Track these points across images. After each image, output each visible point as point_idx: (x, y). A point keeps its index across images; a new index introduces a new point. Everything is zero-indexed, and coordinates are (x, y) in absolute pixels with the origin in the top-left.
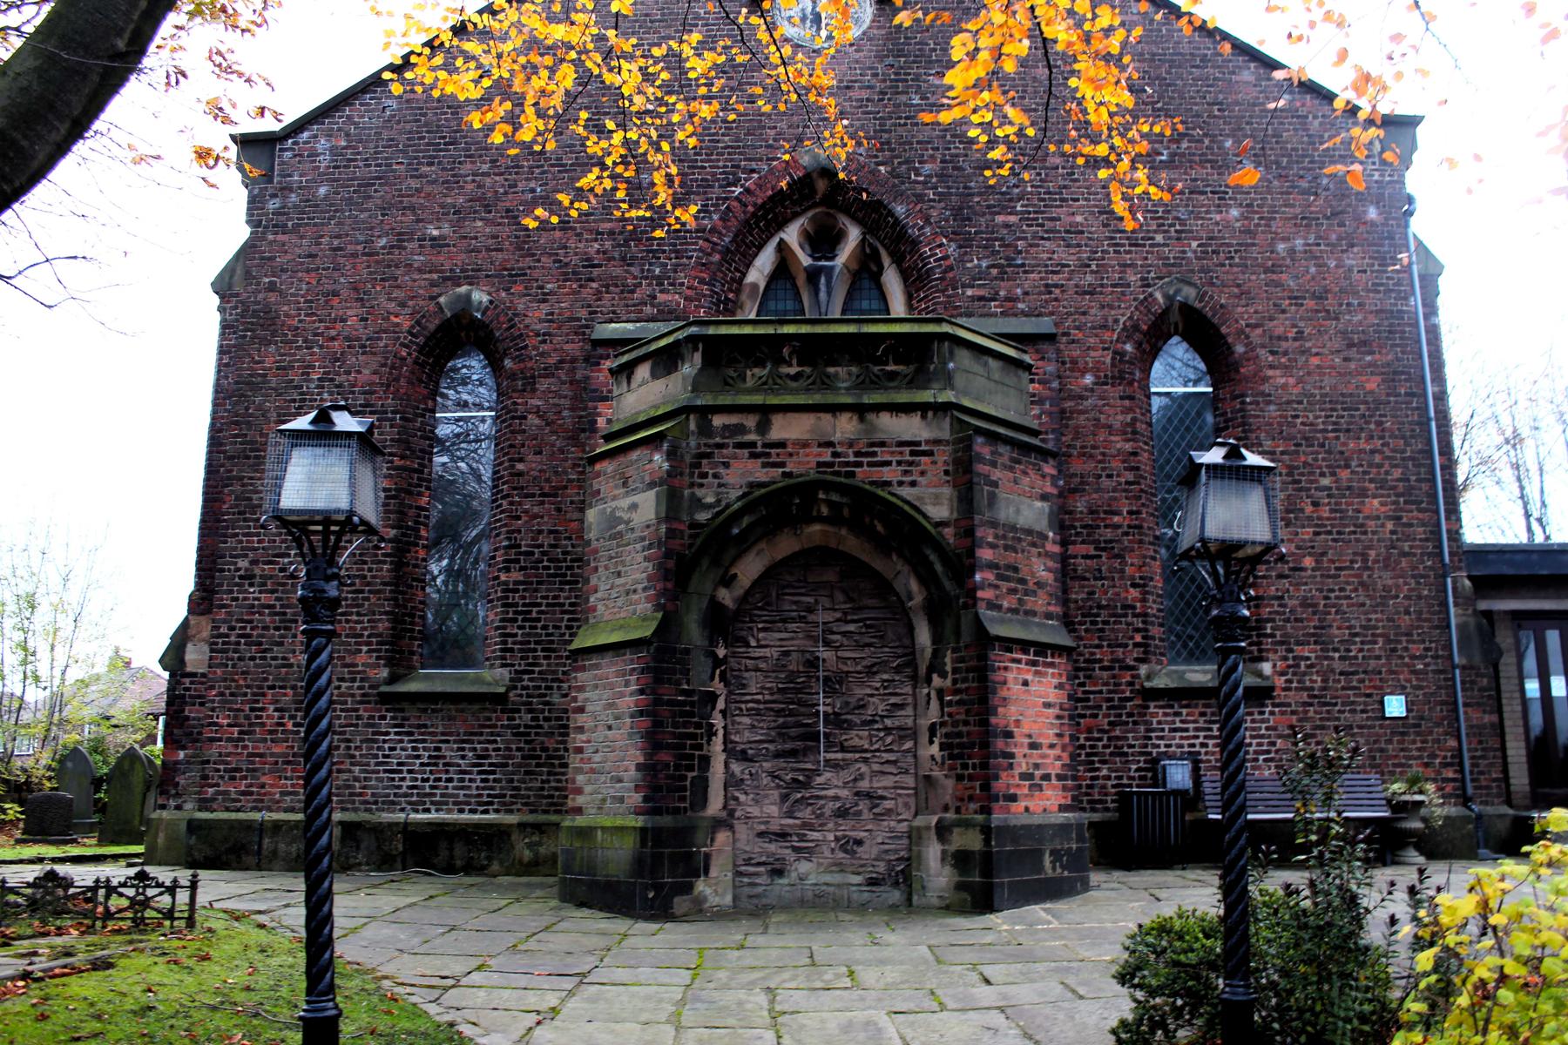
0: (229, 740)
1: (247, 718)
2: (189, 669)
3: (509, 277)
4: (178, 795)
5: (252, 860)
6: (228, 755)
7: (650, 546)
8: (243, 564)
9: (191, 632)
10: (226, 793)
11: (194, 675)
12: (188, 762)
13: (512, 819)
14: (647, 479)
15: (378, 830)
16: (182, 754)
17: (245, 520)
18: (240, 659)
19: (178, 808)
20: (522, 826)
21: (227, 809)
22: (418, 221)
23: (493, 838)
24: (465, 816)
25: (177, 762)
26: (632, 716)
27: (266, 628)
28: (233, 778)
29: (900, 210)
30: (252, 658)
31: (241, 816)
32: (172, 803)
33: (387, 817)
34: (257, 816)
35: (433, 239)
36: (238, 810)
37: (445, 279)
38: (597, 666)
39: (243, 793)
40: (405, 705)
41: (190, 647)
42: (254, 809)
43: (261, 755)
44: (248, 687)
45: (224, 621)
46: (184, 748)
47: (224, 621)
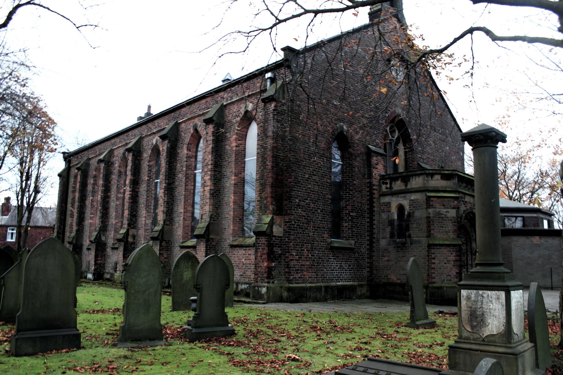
0: (296, 260)
1: (300, 253)
2: (274, 234)
3: (351, 124)
4: (273, 278)
5: (304, 299)
6: (296, 265)
7: (454, 222)
8: (297, 201)
9: (275, 221)
10: (296, 278)
11: (275, 236)
12: (275, 267)
13: (356, 283)
14: (452, 206)
15: (332, 288)
16: (273, 264)
17: (297, 186)
18: (298, 233)
19: (273, 283)
20: (359, 285)
21: (296, 283)
22: (332, 98)
23: (352, 289)
24: (347, 283)
25: (272, 267)
26: (454, 261)
27: (303, 223)
28: (297, 273)
29: (410, 131)
30: (301, 233)
31: (300, 285)
32: (271, 281)
33: (334, 284)
34: (304, 285)
35: (335, 105)
36: (299, 283)
37: (339, 119)
38: (440, 249)
39: (300, 278)
40: (335, 250)
41: (274, 227)
42: (303, 283)
43: (304, 265)
44: (300, 242)
45: (293, 220)
46: (274, 262)
47: (293, 220)
